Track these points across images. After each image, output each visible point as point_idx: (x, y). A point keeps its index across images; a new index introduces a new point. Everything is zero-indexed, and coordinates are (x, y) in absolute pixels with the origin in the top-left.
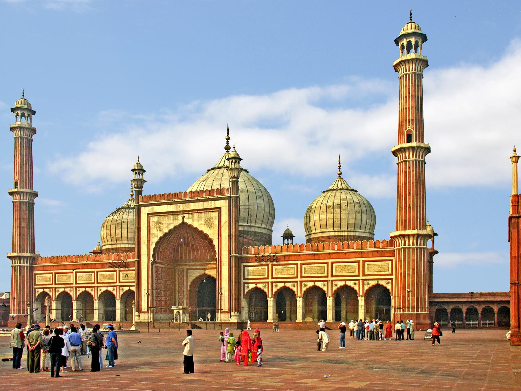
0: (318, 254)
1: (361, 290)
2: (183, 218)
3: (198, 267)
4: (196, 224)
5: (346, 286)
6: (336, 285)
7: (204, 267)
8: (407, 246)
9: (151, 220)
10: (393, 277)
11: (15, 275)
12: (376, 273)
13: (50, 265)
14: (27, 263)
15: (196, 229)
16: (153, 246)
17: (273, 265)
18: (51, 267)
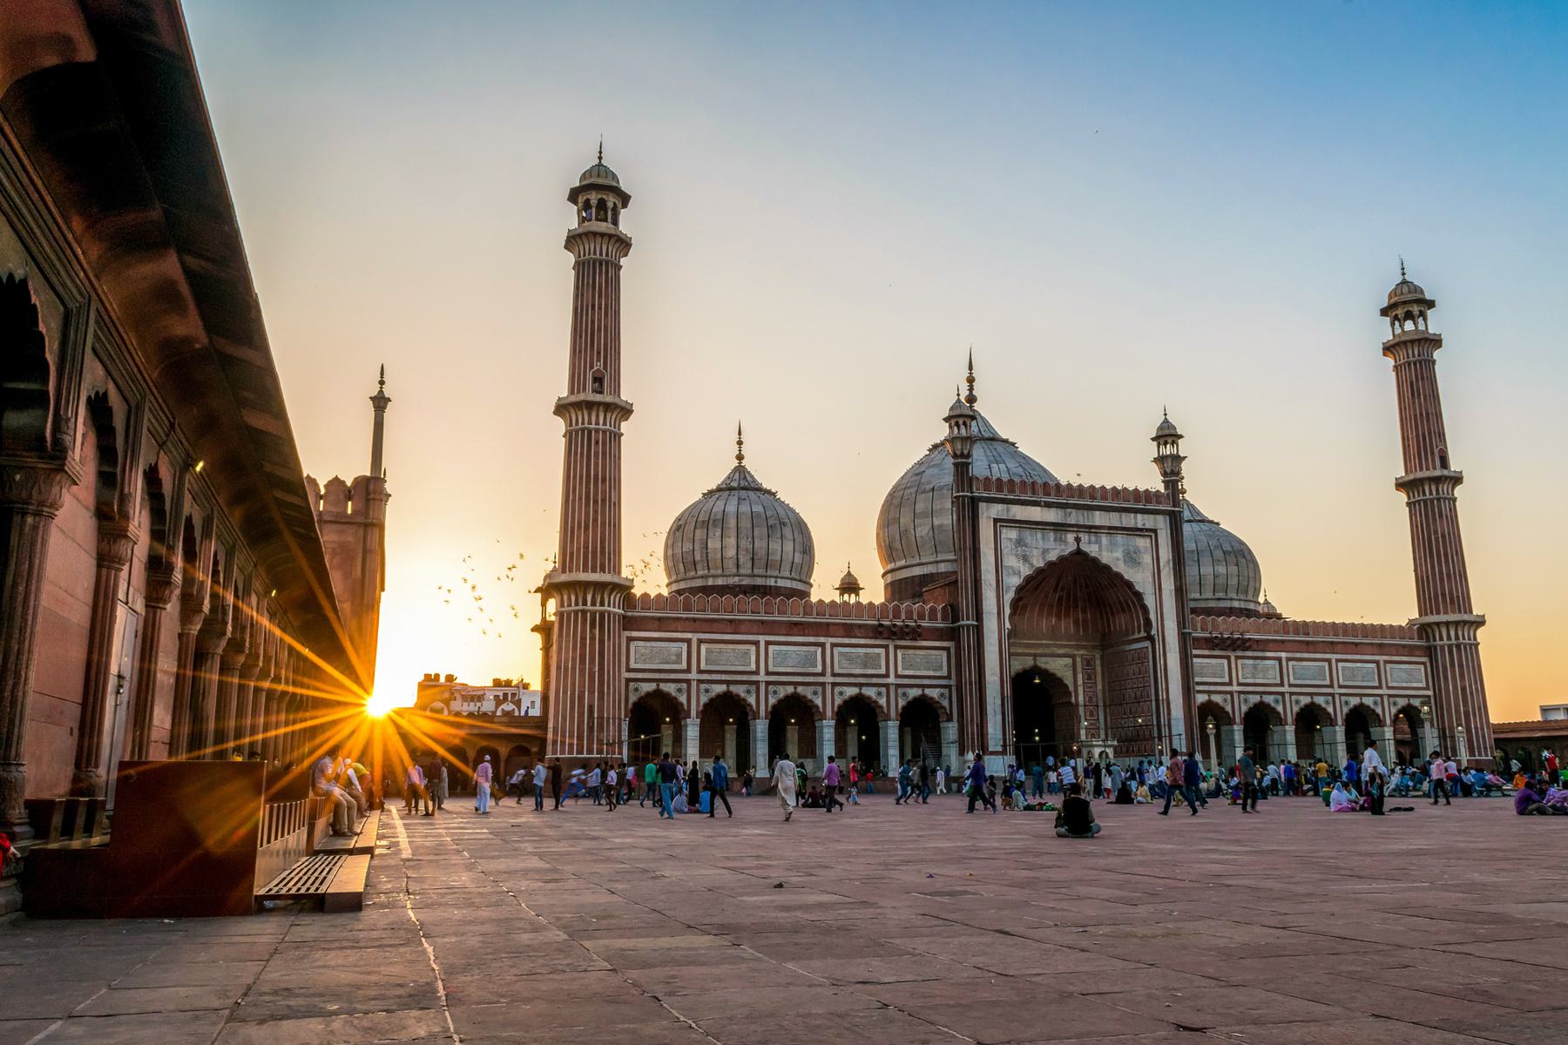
0: (1312, 642)
1: (1388, 713)
2: (1078, 540)
3: (1020, 651)
4: (1106, 558)
5: (1362, 705)
6: (1347, 703)
7: (1033, 651)
8: (1467, 641)
9: (1003, 536)
10: (1430, 693)
11: (593, 639)
12: (1404, 685)
13: (685, 616)
14: (619, 608)
15: (1107, 568)
16: (1009, 596)
17: (1237, 658)
18: (687, 622)
